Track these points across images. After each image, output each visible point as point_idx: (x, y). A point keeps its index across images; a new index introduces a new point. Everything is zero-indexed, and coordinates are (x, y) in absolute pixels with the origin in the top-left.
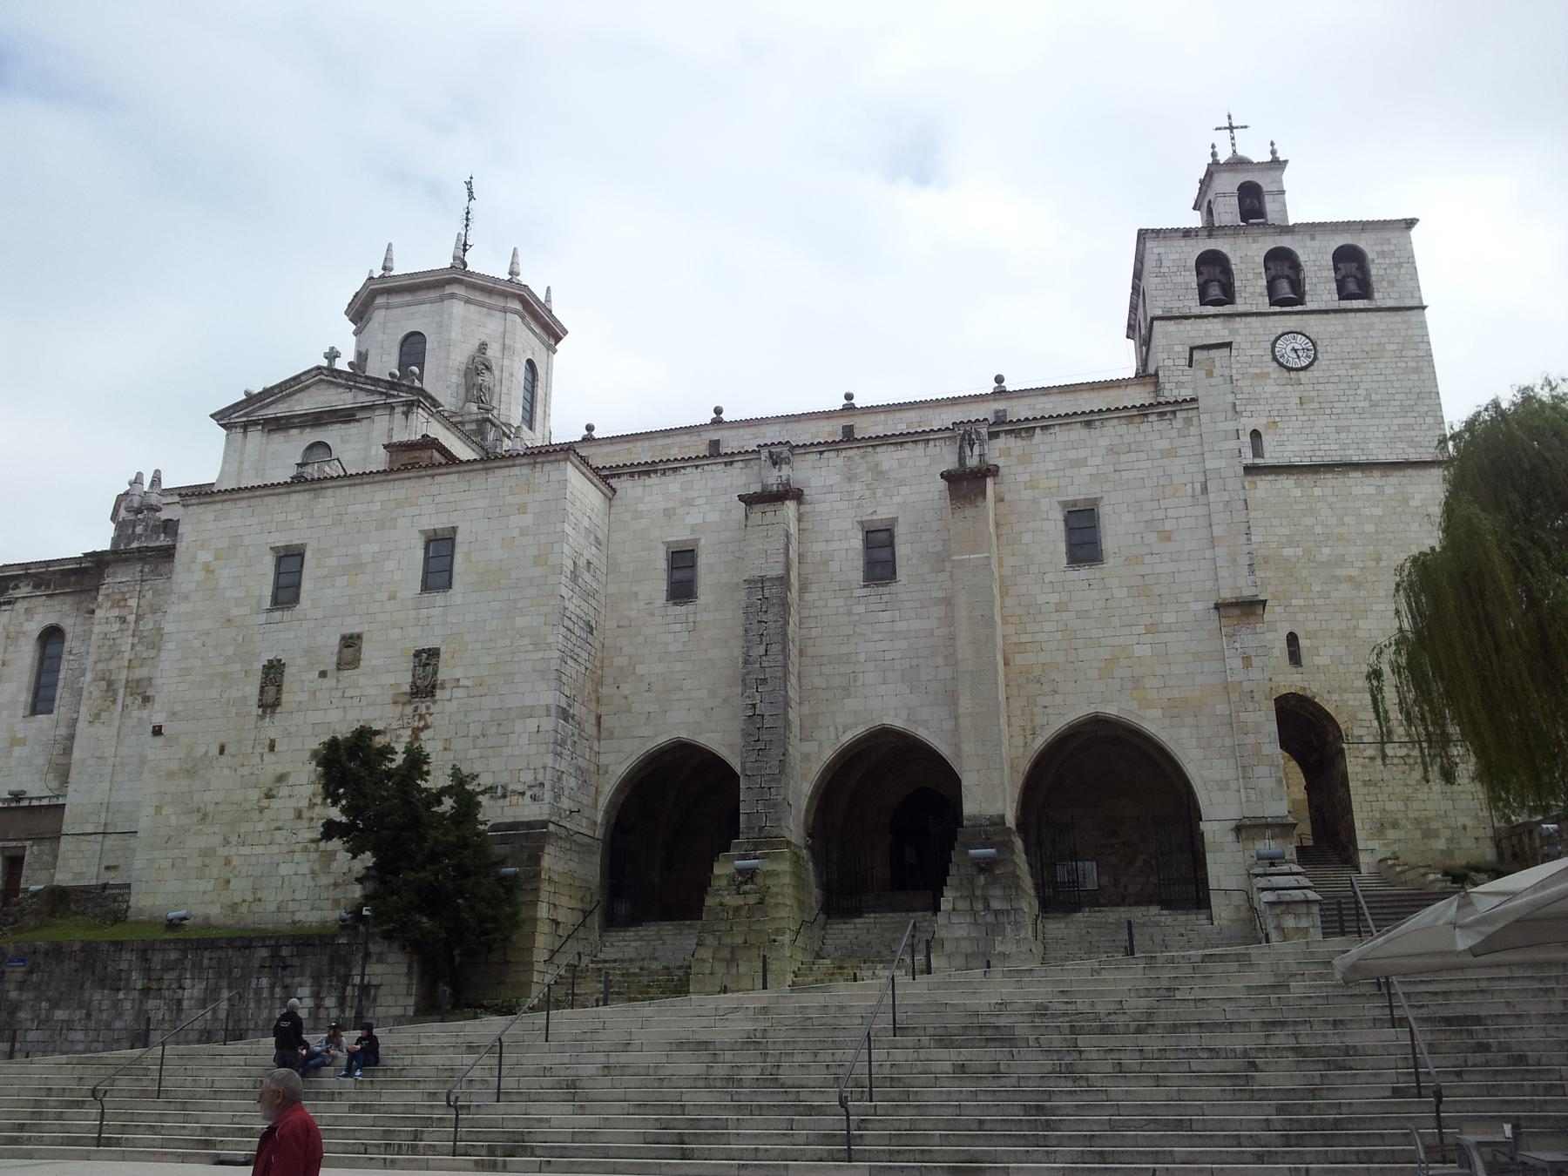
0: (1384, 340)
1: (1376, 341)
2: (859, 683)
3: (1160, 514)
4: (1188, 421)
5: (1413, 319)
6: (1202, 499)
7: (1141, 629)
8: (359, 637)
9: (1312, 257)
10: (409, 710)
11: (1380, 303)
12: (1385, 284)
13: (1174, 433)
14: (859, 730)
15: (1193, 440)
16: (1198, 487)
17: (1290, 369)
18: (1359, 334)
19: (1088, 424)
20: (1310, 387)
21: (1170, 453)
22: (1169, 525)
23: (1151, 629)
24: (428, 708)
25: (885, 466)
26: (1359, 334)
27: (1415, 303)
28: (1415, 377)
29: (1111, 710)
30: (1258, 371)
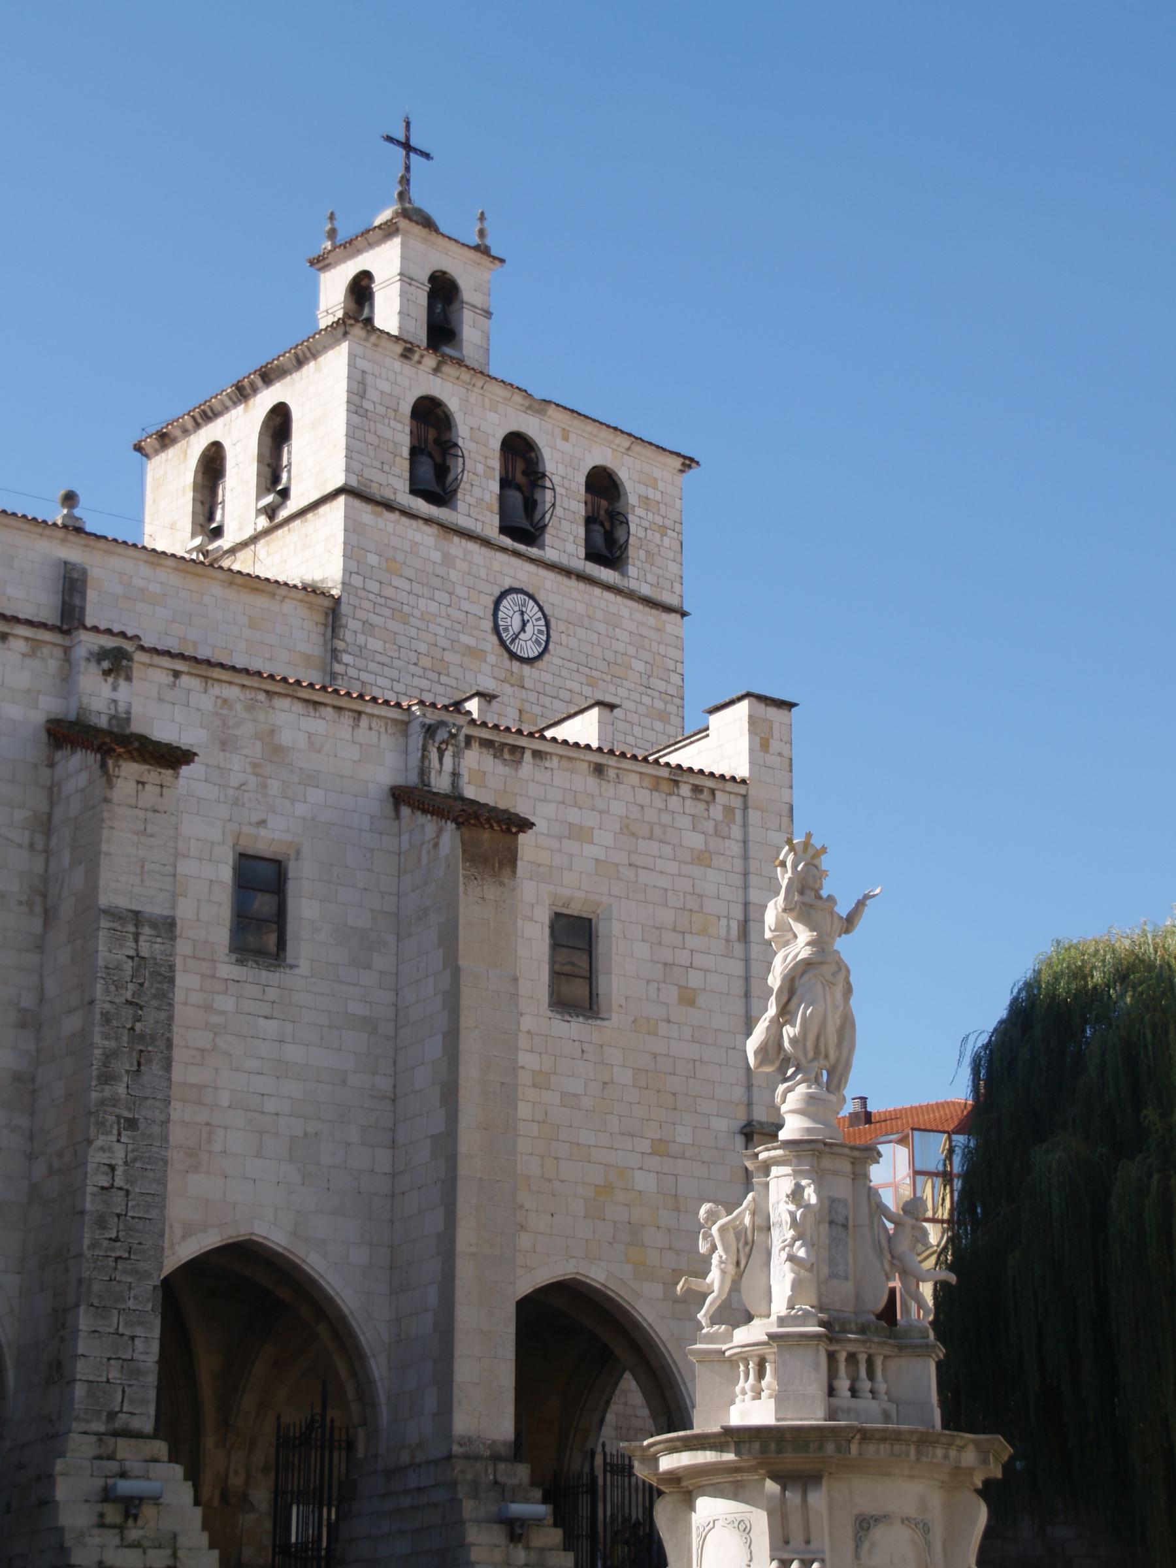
0: (632, 651)
1: (621, 647)
2: (217, 1147)
3: (683, 957)
4: (729, 810)
5: (669, 628)
6: (738, 948)
7: (645, 1145)
9: (561, 470)
11: (633, 585)
12: (642, 553)
13: (709, 827)
14: (211, 1240)
15: (735, 848)
16: (734, 925)
17: (513, 656)
18: (602, 628)
19: (599, 770)
20: (532, 697)
21: (702, 858)
22: (694, 980)
23: (660, 1148)
25: (286, 737)
26: (602, 628)
27: (673, 601)
28: (659, 726)
29: (597, 1275)
30: (471, 642)
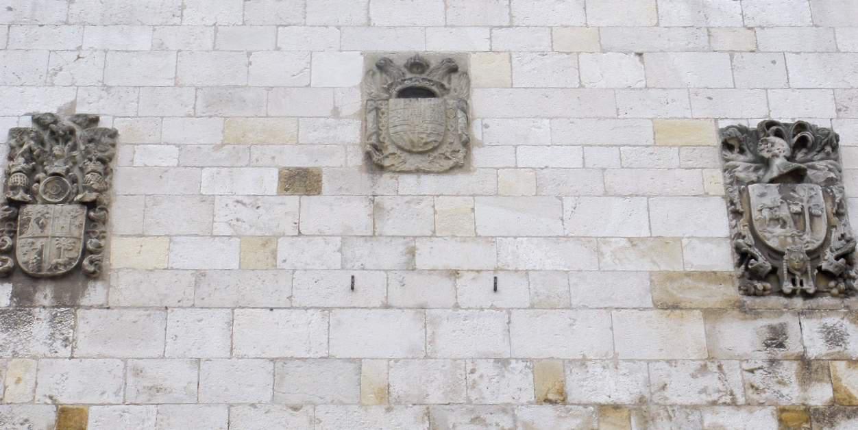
8: (452, 68)
10: (743, 336)
24: (834, 337)
